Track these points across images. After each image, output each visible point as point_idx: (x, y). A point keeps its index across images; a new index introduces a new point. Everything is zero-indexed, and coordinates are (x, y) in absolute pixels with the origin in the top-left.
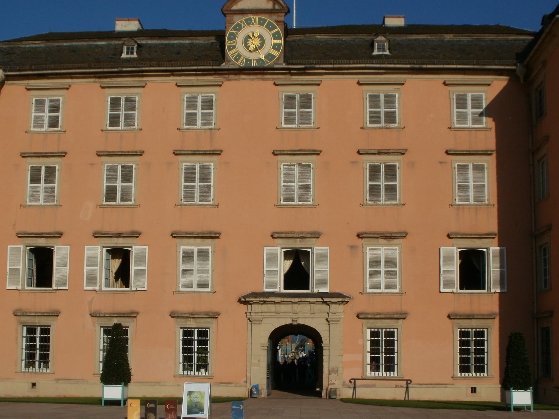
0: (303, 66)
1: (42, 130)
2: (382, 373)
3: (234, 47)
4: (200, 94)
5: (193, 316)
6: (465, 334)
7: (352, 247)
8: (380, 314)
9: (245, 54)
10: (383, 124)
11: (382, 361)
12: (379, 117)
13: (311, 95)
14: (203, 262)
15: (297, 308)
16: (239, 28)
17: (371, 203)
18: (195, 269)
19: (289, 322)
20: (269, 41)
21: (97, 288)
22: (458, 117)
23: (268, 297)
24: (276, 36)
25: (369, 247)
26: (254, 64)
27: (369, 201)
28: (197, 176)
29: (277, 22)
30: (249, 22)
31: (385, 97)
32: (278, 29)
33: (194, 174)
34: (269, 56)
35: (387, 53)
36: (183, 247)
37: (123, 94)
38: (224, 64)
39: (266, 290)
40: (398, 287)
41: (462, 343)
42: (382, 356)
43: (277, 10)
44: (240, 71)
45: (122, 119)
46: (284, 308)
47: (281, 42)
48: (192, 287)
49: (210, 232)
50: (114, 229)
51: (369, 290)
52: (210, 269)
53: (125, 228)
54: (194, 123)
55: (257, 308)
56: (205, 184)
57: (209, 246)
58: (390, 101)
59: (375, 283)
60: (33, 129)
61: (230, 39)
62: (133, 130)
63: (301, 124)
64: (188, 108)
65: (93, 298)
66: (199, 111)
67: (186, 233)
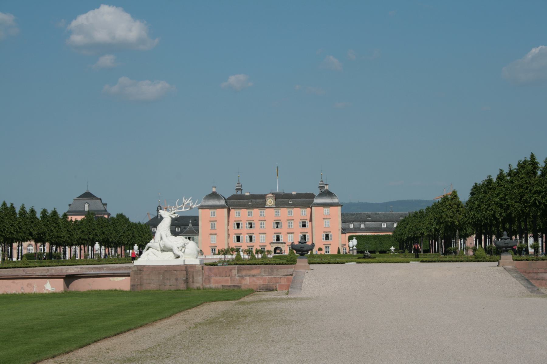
4: (262, 211)
14: (264, 238)
16: (268, 200)
18: (263, 239)
24: (274, 201)
25: (289, 235)
26: (271, 206)
30: (269, 199)
34: (273, 205)
35: (291, 202)
36: (261, 235)
37: (250, 211)
45: (250, 215)
46: (276, 245)
47: (274, 202)
57: (264, 235)
58: (291, 212)
66: (262, 214)
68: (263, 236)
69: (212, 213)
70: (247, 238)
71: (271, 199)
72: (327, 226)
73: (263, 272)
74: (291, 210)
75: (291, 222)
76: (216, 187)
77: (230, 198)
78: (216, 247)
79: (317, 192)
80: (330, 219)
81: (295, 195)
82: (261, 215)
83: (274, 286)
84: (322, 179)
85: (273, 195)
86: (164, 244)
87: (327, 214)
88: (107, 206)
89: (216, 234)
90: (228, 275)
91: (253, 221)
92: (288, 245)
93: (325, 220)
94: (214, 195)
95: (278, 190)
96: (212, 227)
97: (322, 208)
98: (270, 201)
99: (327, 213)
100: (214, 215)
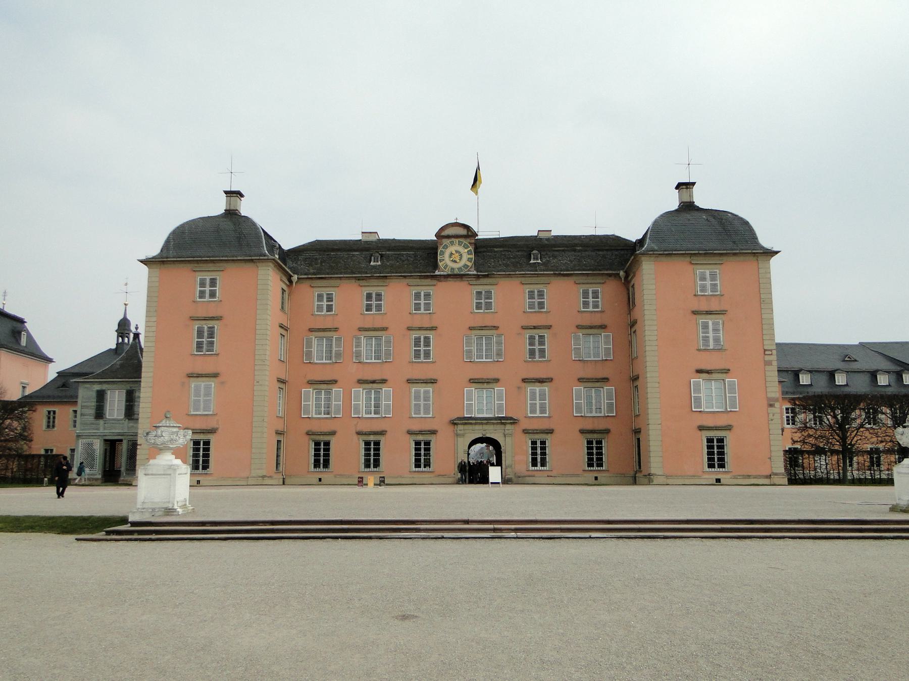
0: (486, 273)
1: (323, 313)
2: (539, 468)
3: (443, 260)
5: (421, 432)
6: (590, 442)
7: (519, 388)
8: (537, 430)
10: (537, 309)
11: (539, 460)
12: (534, 305)
13: (491, 291)
14: (426, 399)
15: (485, 427)
16: (446, 247)
17: (530, 360)
18: (422, 403)
19: (481, 436)
20: (465, 257)
21: (360, 416)
22: (583, 304)
23: (468, 420)
24: (469, 253)
25: (529, 388)
27: (529, 358)
28: (422, 343)
29: (470, 243)
30: (452, 243)
31: (538, 292)
32: (470, 248)
33: (420, 342)
34: (466, 266)
35: (539, 261)
37: (374, 291)
38: (437, 271)
39: (465, 416)
40: (548, 413)
41: (588, 448)
42: (539, 457)
43: (470, 236)
44: (447, 277)
46: (477, 427)
47: (472, 256)
48: (420, 414)
49: (431, 379)
50: (370, 378)
51: (529, 415)
52: (431, 402)
53: (377, 377)
54: (419, 309)
55: (460, 427)
56: (427, 348)
57: (430, 388)
58: (541, 295)
59: (533, 411)
60: (316, 313)
61: (440, 255)
62: (381, 314)
63: (486, 310)
64: (415, 300)
65: (358, 422)
66: (422, 302)
67: (416, 380)
68: (422, 390)
69: (203, 284)
70: (357, 399)
74: (541, 287)
78: (213, 431)
82: (417, 307)
87: (709, 293)
89: (215, 375)
91: (385, 329)
92: (526, 432)
93: (701, 320)
96: (199, 346)
98: (456, 252)
99: (709, 287)
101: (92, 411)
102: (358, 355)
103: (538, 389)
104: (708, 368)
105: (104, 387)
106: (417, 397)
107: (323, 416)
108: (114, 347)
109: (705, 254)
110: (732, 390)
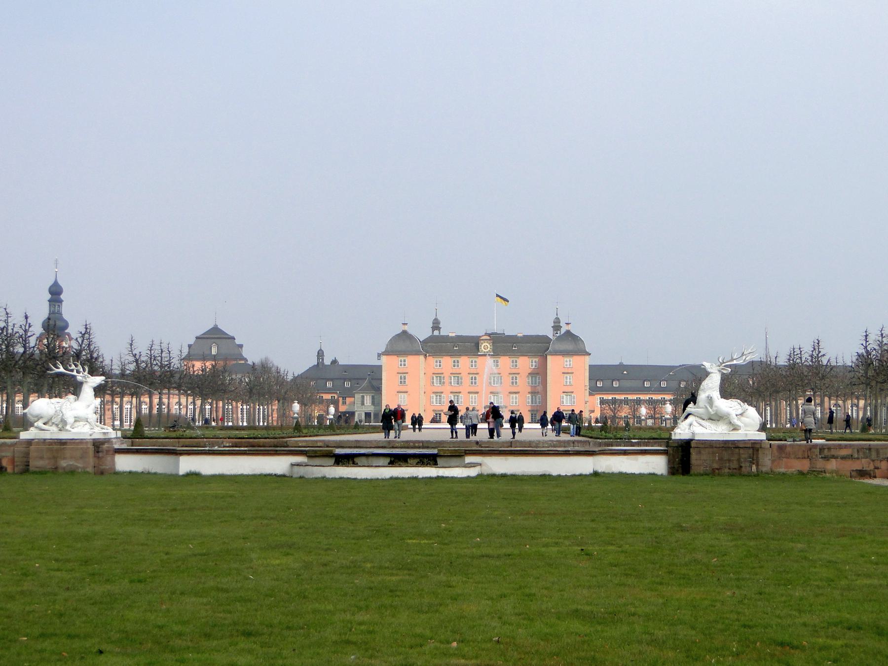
6: (532, 414)
7: (508, 395)
9: (484, 350)
14: (475, 399)
16: (482, 344)
24: (490, 346)
30: (484, 342)
34: (489, 351)
37: (456, 359)
41: (532, 417)
50: (455, 391)
53: (458, 391)
58: (516, 362)
69: (401, 361)
71: (487, 342)
72: (568, 384)
73: (856, 453)
75: (516, 377)
76: (407, 324)
77: (425, 342)
79: (550, 334)
80: (572, 373)
81: (521, 337)
82: (472, 366)
83: (872, 473)
84: (557, 315)
85: (490, 337)
86: (717, 411)
88: (243, 348)
89: (407, 392)
90: (806, 456)
91: (460, 374)
93: (565, 375)
94: (404, 336)
95: (496, 329)
97: (560, 357)
100: (405, 365)
101: (360, 403)
102: (451, 383)
103: (514, 396)
104: (566, 391)
105: (364, 394)
106: (472, 399)
107: (438, 404)
108: (316, 364)
109: (569, 352)
110: (574, 398)
